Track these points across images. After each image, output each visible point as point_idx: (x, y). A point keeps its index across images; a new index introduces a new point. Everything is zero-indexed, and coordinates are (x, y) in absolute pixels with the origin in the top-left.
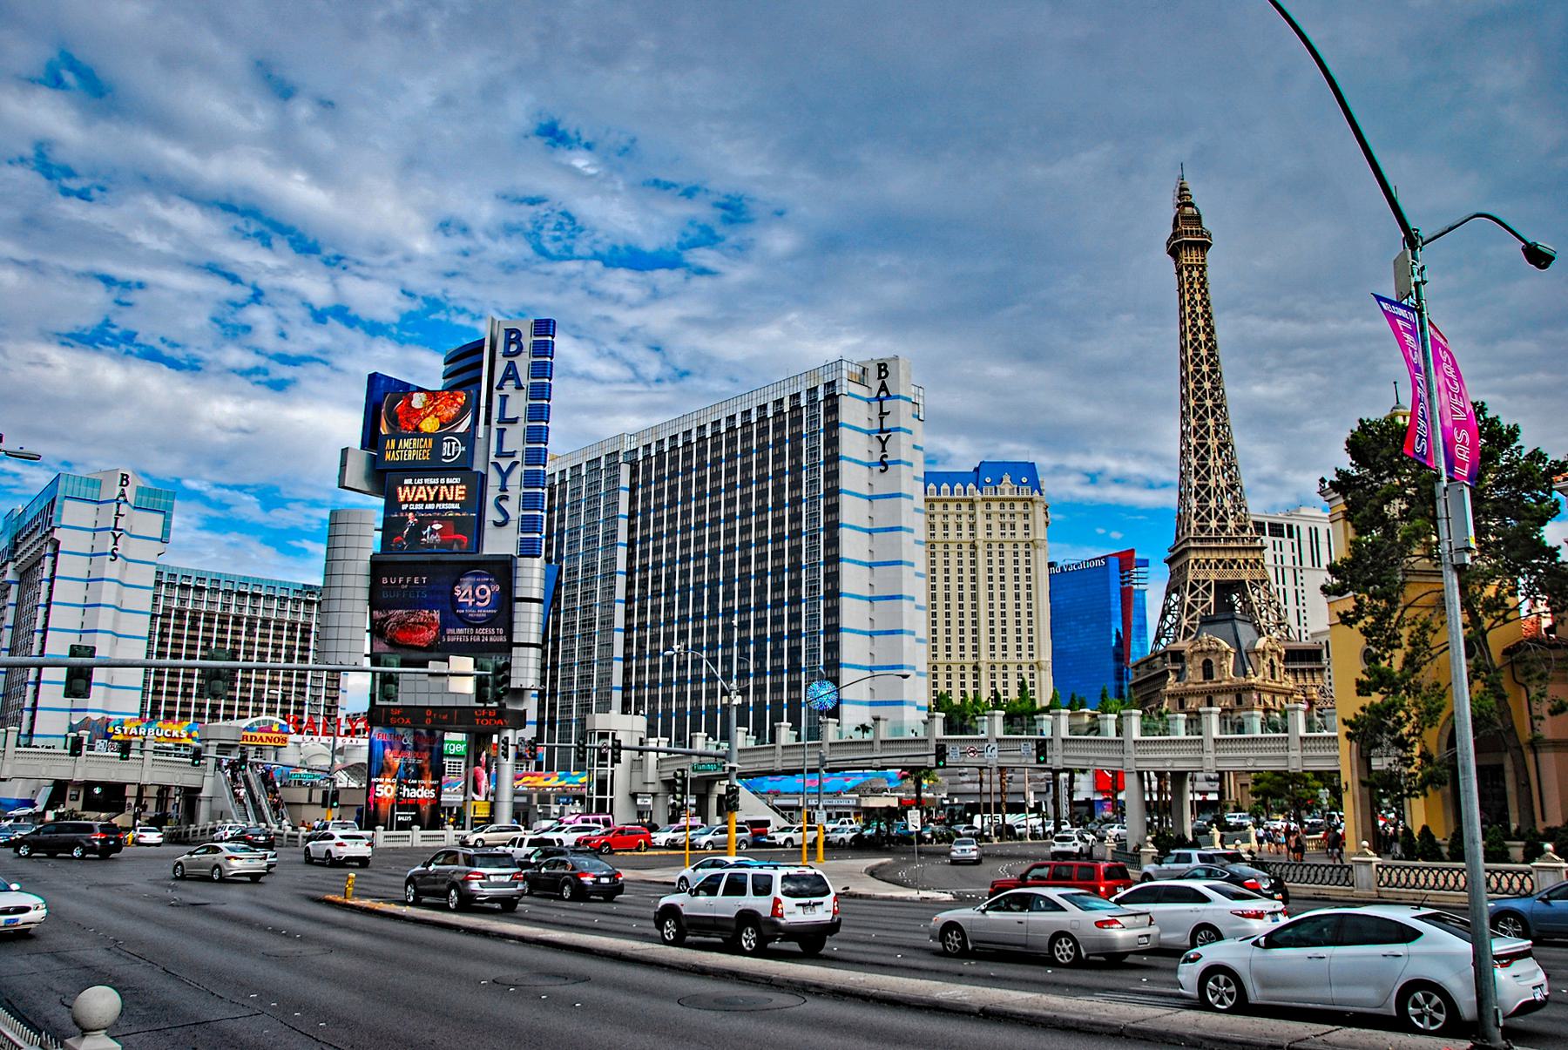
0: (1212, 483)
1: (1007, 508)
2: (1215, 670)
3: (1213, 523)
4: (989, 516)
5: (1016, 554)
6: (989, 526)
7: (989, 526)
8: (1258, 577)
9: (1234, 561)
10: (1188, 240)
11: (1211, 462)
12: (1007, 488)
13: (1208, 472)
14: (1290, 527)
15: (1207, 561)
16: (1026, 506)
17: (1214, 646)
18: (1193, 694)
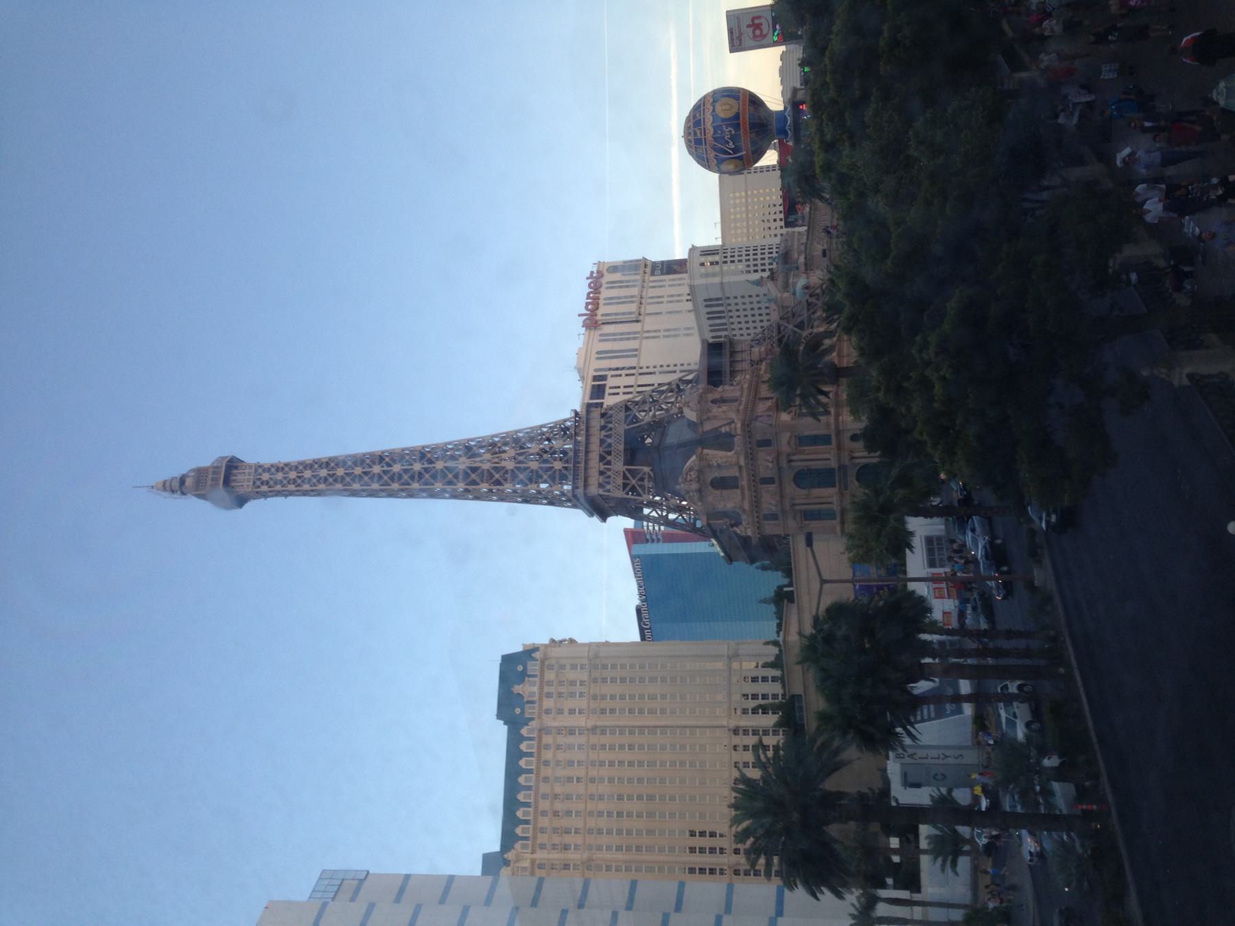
0: (510, 465)
1: (552, 689)
2: (725, 473)
3: (558, 465)
4: (560, 712)
5: (604, 680)
6: (572, 712)
7: (572, 712)
8: (622, 415)
9: (602, 442)
10: (229, 482)
11: (486, 466)
12: (528, 689)
13: (497, 469)
14: (595, 378)
15: (601, 473)
16: (551, 667)
17: (693, 474)
18: (756, 503)
